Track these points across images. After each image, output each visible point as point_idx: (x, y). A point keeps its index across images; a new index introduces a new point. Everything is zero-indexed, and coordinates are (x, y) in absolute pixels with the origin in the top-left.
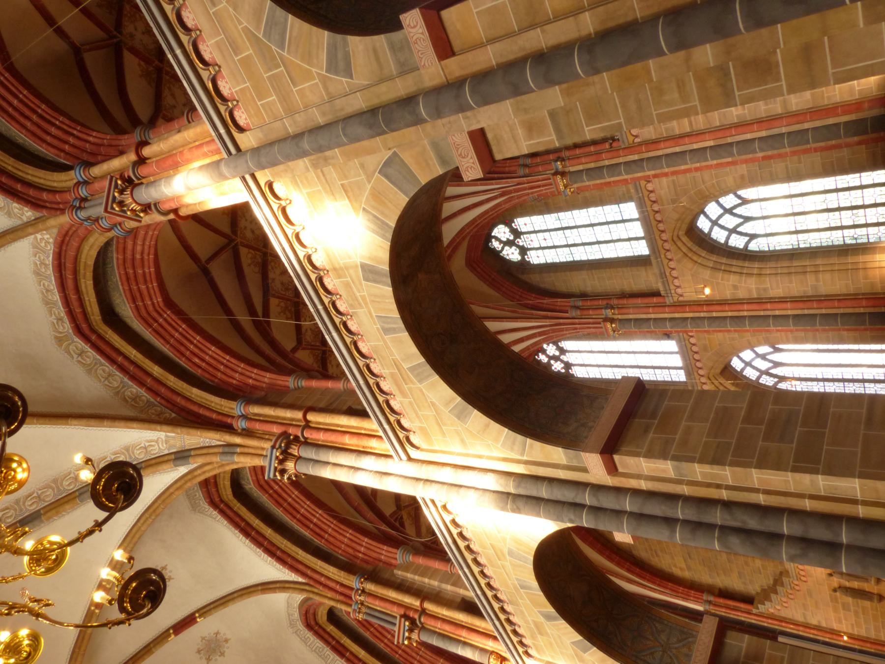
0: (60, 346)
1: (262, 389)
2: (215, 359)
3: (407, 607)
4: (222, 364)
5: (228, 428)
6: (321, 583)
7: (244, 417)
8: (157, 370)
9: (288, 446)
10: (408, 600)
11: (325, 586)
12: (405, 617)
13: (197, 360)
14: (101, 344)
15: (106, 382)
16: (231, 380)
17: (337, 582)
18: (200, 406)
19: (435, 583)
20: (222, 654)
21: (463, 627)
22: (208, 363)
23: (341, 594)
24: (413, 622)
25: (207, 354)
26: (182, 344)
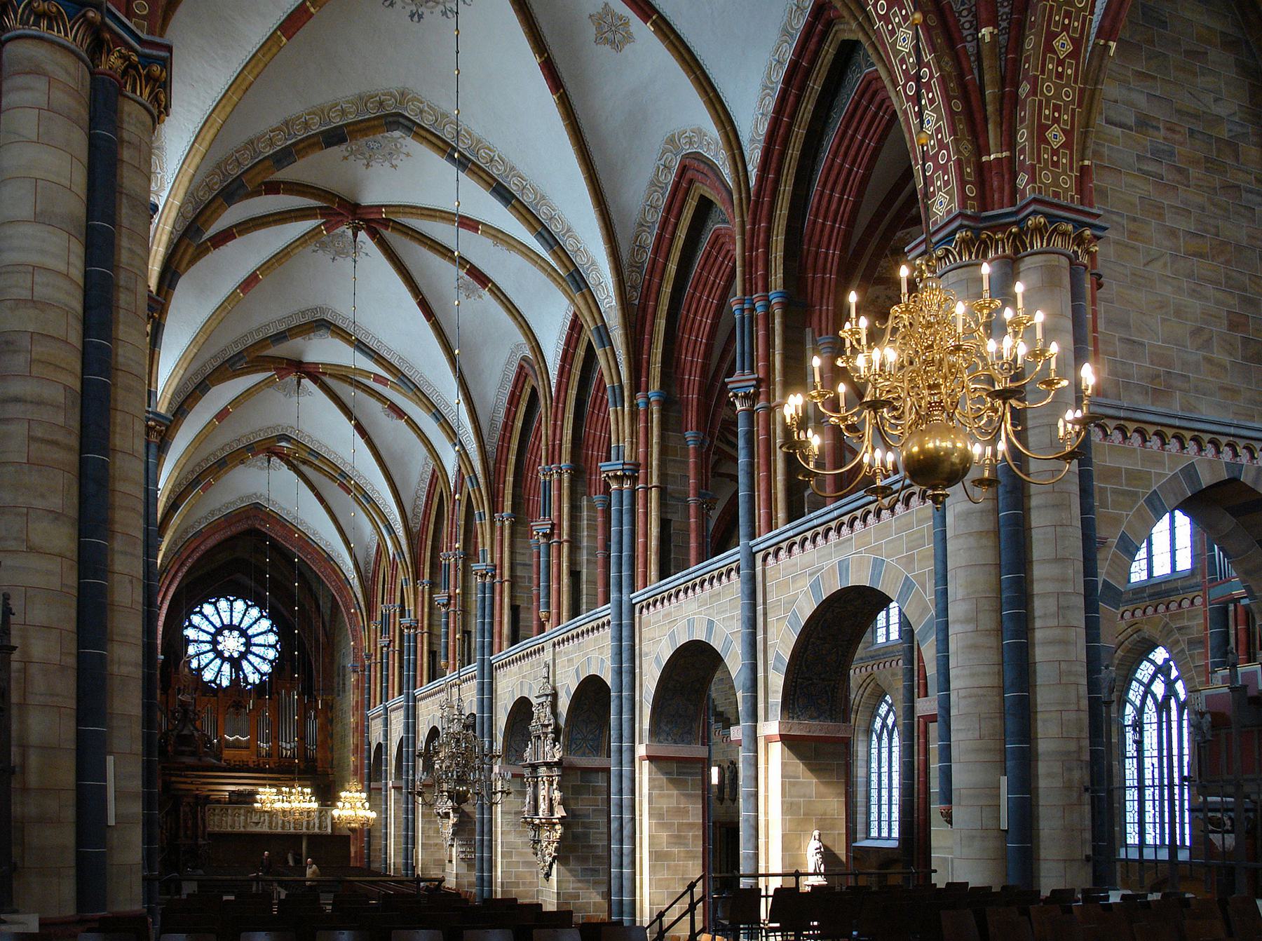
0: (667, 143)
1: (682, 394)
2: (700, 325)
3: (560, 525)
4: (697, 337)
5: (636, 387)
6: (556, 421)
7: (648, 403)
8: (672, 267)
9: (628, 477)
10: (565, 524)
11: (555, 424)
12: (553, 525)
13: (694, 306)
14: (680, 195)
15: (647, 208)
16: (684, 352)
17: (561, 440)
18: (651, 334)
19: (585, 543)
20: (468, 297)
21: (559, 584)
22: (694, 319)
23: (554, 445)
24: (552, 534)
25: (702, 317)
26: (705, 285)
